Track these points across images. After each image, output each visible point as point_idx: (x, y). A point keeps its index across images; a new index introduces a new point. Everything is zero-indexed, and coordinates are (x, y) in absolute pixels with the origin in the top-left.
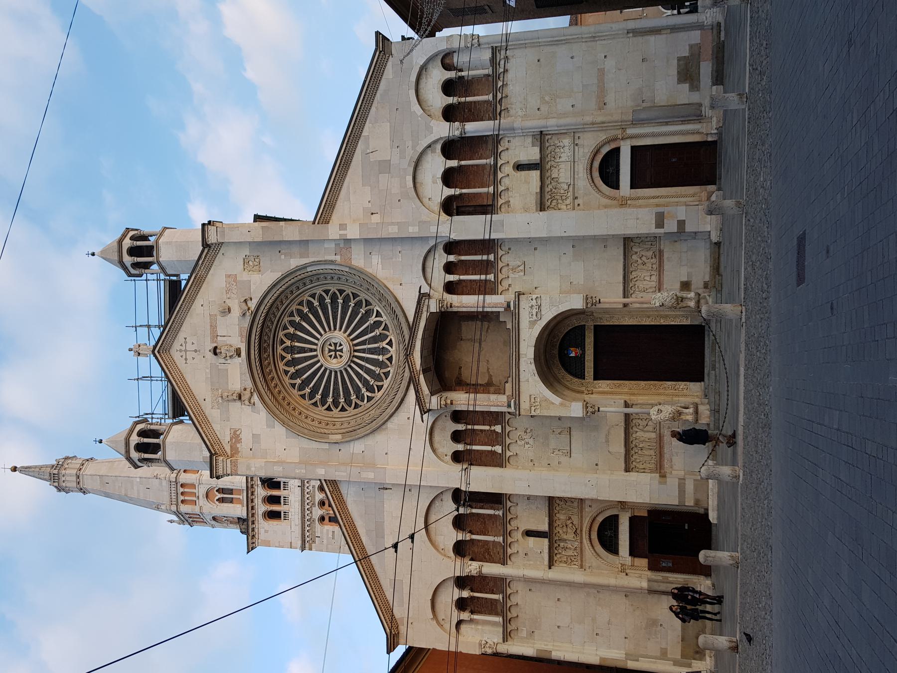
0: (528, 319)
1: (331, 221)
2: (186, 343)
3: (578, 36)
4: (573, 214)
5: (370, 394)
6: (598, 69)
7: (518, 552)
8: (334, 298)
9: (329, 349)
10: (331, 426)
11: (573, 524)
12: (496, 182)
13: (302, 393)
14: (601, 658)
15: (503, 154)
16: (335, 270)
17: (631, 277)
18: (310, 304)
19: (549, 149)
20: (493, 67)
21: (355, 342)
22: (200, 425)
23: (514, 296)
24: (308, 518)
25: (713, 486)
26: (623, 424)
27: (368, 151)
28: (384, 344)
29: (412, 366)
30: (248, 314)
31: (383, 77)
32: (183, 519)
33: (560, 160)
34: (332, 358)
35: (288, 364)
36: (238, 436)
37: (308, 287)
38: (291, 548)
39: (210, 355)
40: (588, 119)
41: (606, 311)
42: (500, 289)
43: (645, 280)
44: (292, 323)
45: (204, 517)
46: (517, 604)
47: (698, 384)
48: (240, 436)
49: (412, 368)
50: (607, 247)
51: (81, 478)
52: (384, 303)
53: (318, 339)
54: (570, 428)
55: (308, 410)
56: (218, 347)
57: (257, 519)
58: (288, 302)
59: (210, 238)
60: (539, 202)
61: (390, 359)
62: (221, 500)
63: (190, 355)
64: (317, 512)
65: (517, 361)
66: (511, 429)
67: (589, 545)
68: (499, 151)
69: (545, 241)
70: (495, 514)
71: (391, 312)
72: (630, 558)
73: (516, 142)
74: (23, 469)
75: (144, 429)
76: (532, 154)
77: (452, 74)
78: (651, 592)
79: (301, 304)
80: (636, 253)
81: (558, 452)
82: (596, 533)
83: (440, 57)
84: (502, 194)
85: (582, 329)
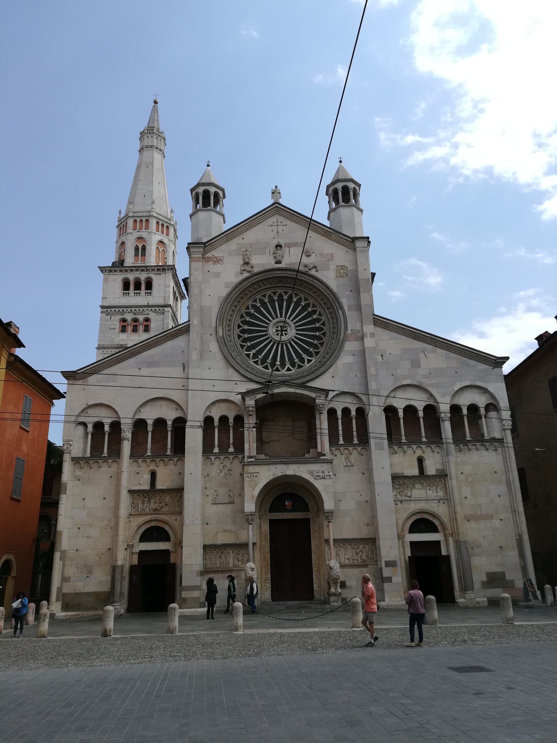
0: (314, 470)
1: (375, 327)
2: (283, 225)
3: (514, 499)
4: (392, 500)
5: (251, 355)
6: (493, 515)
7: (140, 467)
8: (319, 329)
10: (227, 328)
11: (162, 507)
12: (410, 444)
13: (250, 307)
14: (61, 532)
15: (429, 448)
16: (341, 330)
17: (347, 545)
18: (314, 312)
19: (435, 482)
20: (490, 440)
21: (288, 344)
22: (225, 236)
23: (329, 459)
24: (125, 310)
25: (199, 612)
26: (239, 542)
27: (426, 353)
28: (288, 365)
29: (276, 386)
30: (306, 269)
31: (478, 363)
32: (122, 221)
33: (427, 490)
34: (276, 328)
35: (270, 296)
36: (218, 262)
37: (327, 311)
38: (102, 298)
39: (275, 242)
40: (458, 509)
41: (321, 528)
42: (333, 449)
43: (345, 555)
44: (300, 300)
45: (124, 235)
46: (101, 467)
47: (270, 597)
49: (275, 386)
50: (367, 526)
51: (151, 149)
52: (318, 365)
53: (289, 318)
54: (234, 503)
55: (238, 311)
57: (123, 273)
58: (316, 297)
59: (359, 242)
60: (397, 475)
61: (277, 370)
62: (137, 249)
63: (275, 228)
64: (129, 317)
65: (284, 462)
66: (231, 459)
67: (147, 520)
68: (431, 446)
69: (370, 481)
70: (168, 449)
71: (312, 370)
72: (138, 551)
73: (438, 457)
74: (156, 108)
75: (219, 196)
76: (431, 469)
77: (483, 411)
78: (114, 568)
80: (364, 548)
81: (215, 494)
82: (155, 525)
83: (494, 402)
84: (401, 449)
85: (306, 509)
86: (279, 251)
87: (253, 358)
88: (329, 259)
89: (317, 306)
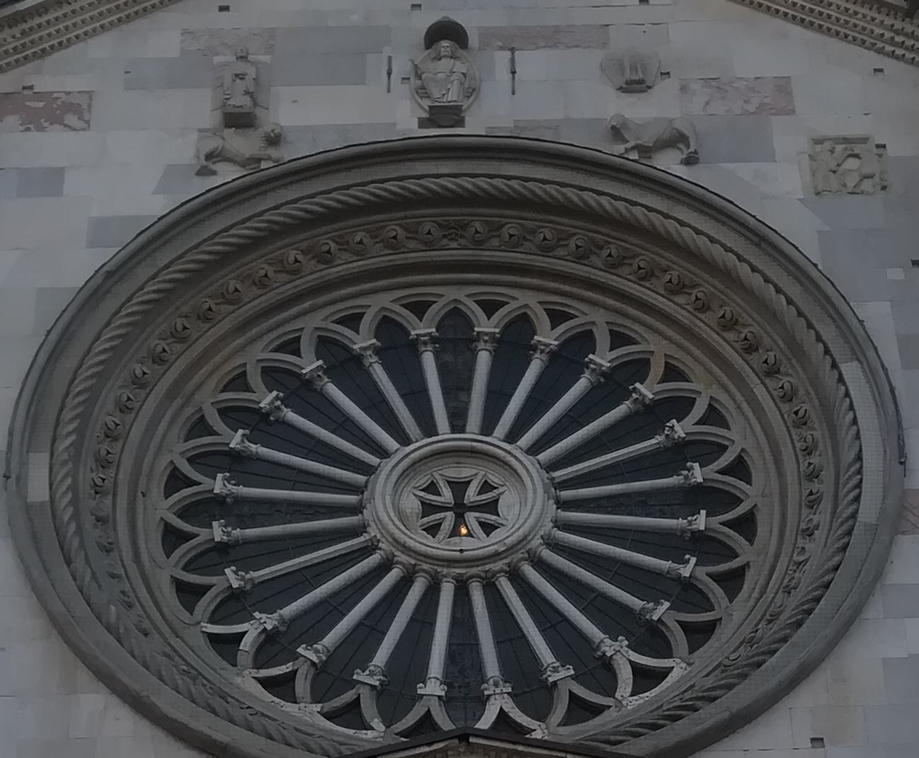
9: (469, 482)
13: (255, 379)
30: (619, 148)
34: (422, 494)
35: (388, 327)
37: (760, 391)
39: (425, 20)
48: (57, 126)
55: (170, 395)
56: (461, 52)
58: (682, 316)
79: (672, 373)
86: (446, 64)
87: (263, 657)
88: (761, 107)
89: (694, 369)
